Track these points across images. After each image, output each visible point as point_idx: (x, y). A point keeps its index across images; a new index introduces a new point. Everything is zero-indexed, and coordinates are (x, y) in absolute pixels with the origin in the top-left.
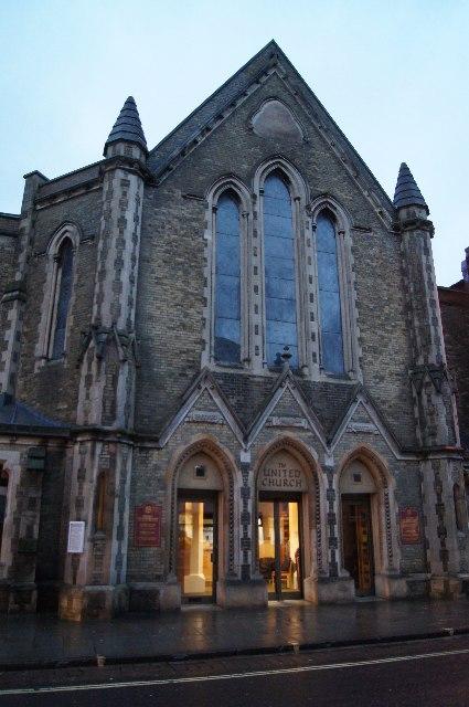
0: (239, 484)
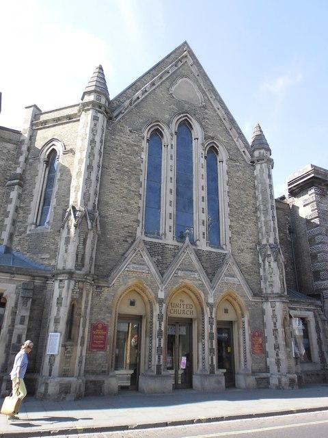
0: (156, 313)
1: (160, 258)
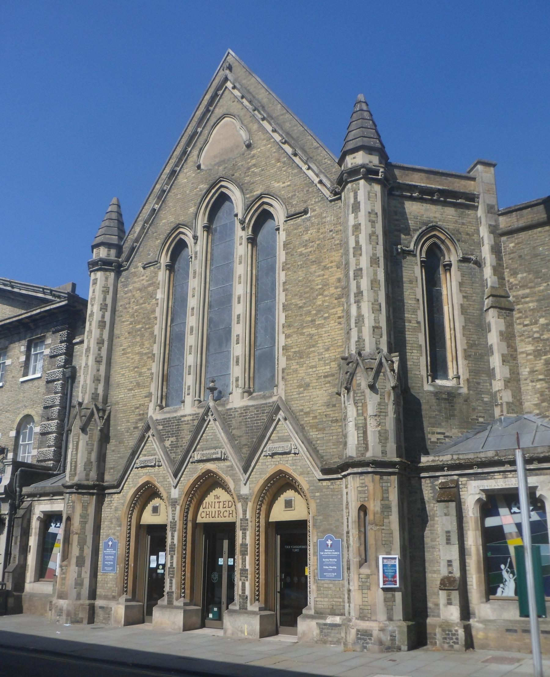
1: (173, 439)
